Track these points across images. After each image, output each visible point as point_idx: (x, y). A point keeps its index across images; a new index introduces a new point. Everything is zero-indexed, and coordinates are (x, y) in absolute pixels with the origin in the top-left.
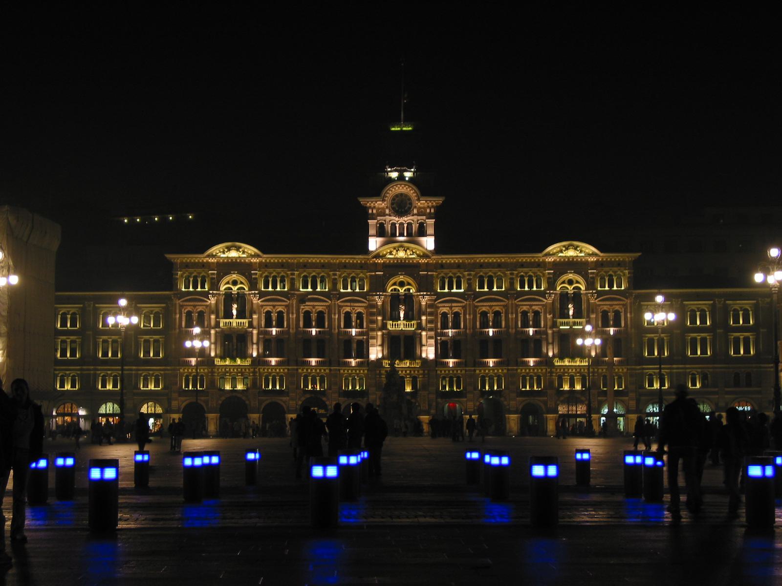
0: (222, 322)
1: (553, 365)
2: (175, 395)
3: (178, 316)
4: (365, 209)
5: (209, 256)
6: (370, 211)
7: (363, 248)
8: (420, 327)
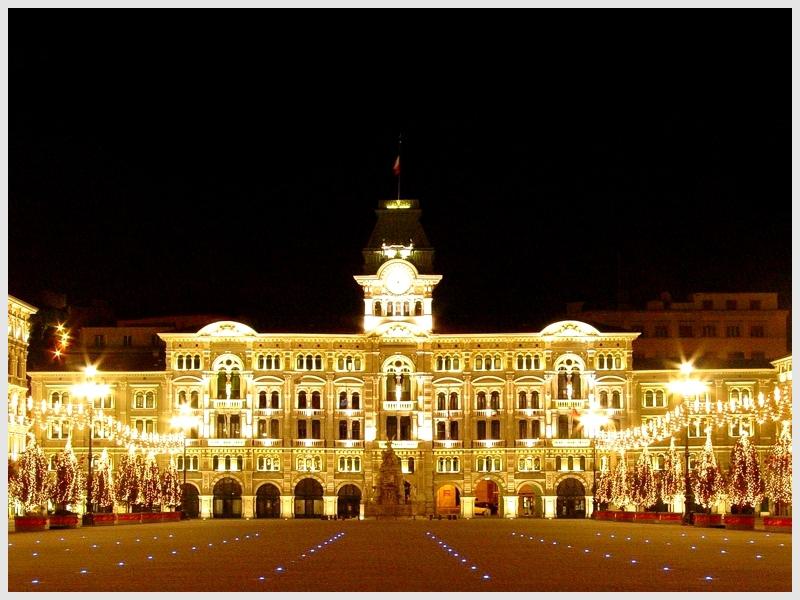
6: (366, 290)
7: (356, 328)
8: (417, 407)
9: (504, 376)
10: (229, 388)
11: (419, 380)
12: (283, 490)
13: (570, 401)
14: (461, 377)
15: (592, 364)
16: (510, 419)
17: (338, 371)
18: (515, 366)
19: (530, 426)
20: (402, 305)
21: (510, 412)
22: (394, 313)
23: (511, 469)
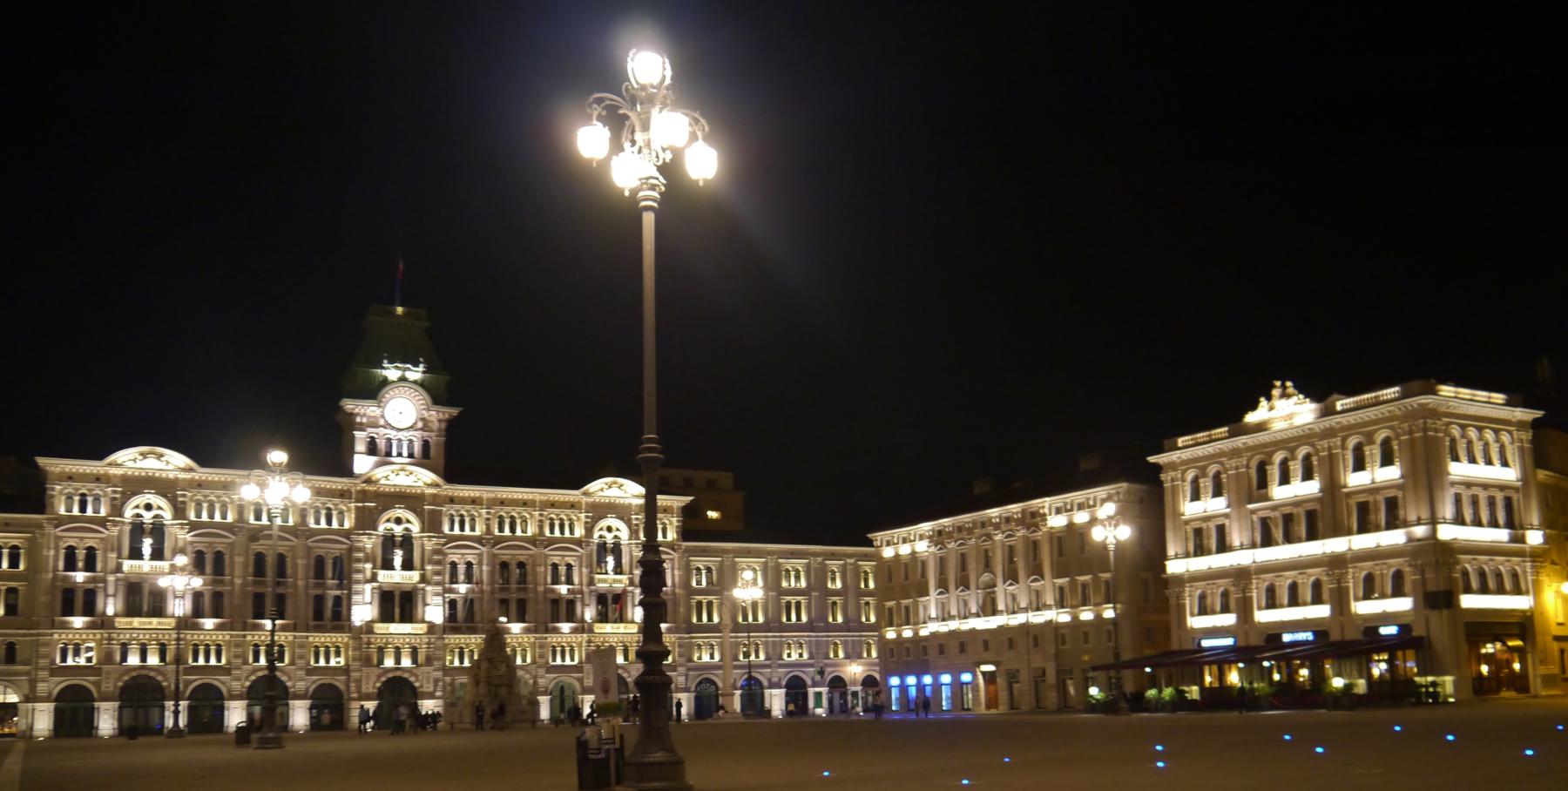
0: (128, 565)
1: (591, 631)
2: (43, 674)
3: (52, 552)
4: (352, 415)
5: (110, 464)
6: (358, 420)
7: (346, 470)
8: (423, 579)
9: (533, 541)
10: (147, 545)
11: (425, 543)
12: (229, 691)
13: (611, 576)
14: (479, 540)
15: (637, 532)
16: (541, 597)
17: (312, 525)
18: (547, 533)
19: (563, 607)
20: (405, 445)
21: (541, 589)
22: (394, 453)
23: (300, 662)
